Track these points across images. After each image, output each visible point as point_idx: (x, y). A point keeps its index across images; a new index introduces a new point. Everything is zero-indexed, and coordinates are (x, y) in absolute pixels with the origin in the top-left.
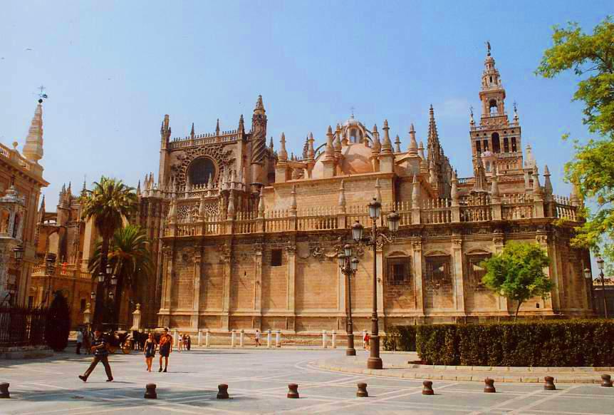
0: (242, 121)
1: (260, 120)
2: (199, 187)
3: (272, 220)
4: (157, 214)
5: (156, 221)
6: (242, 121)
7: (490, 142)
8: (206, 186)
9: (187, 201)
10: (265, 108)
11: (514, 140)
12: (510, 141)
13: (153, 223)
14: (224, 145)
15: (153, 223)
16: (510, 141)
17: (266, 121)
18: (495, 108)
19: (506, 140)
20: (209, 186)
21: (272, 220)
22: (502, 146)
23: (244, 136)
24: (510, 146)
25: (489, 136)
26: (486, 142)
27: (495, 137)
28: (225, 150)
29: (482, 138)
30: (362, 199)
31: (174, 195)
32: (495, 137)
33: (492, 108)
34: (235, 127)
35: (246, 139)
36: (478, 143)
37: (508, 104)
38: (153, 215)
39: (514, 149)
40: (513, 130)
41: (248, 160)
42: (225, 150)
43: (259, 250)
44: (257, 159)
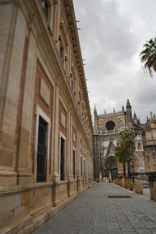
0: (123, 108)
1: (129, 107)
2: (110, 130)
4: (98, 140)
5: (98, 142)
6: (123, 108)
8: (113, 130)
9: (107, 135)
10: (130, 103)
13: (97, 143)
14: (117, 116)
15: (97, 143)
17: (131, 107)
20: (114, 130)
23: (125, 113)
28: (118, 117)
31: (102, 134)
34: (121, 110)
35: (125, 113)
38: (96, 141)
41: (127, 121)
42: (118, 117)
43: (154, 150)
44: (130, 120)
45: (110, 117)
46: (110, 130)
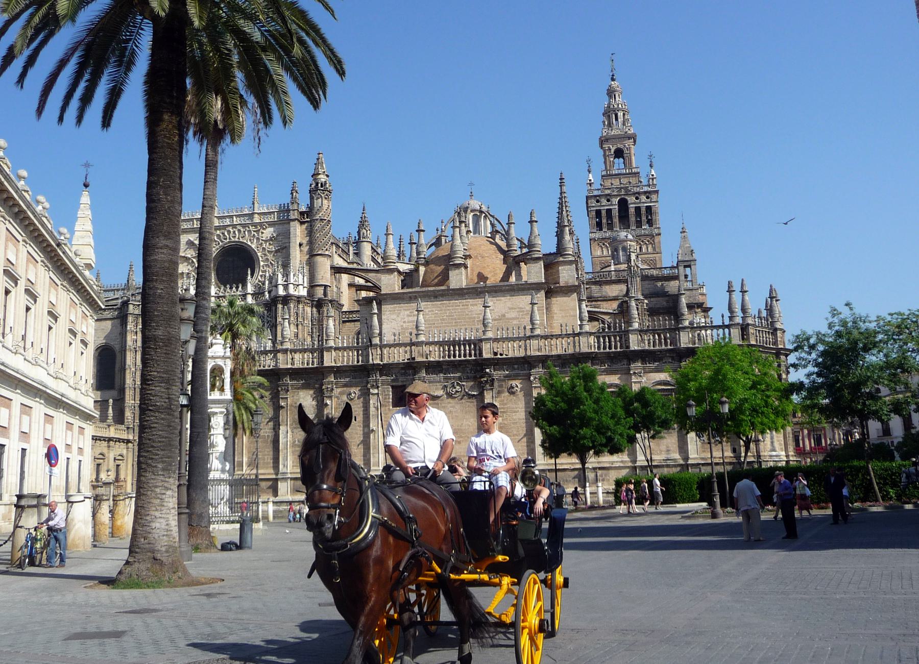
0: (293, 191)
2: (231, 288)
3: (390, 346)
7: (615, 213)
11: (649, 209)
12: (643, 210)
16: (643, 210)
18: (621, 160)
19: (638, 209)
21: (390, 346)
22: (632, 219)
24: (644, 218)
25: (616, 201)
26: (609, 212)
27: (623, 204)
29: (604, 205)
30: (504, 316)
32: (623, 204)
33: (616, 160)
36: (598, 213)
37: (637, 156)
39: (650, 223)
40: (648, 194)
45: (234, 226)
46: (231, 288)
